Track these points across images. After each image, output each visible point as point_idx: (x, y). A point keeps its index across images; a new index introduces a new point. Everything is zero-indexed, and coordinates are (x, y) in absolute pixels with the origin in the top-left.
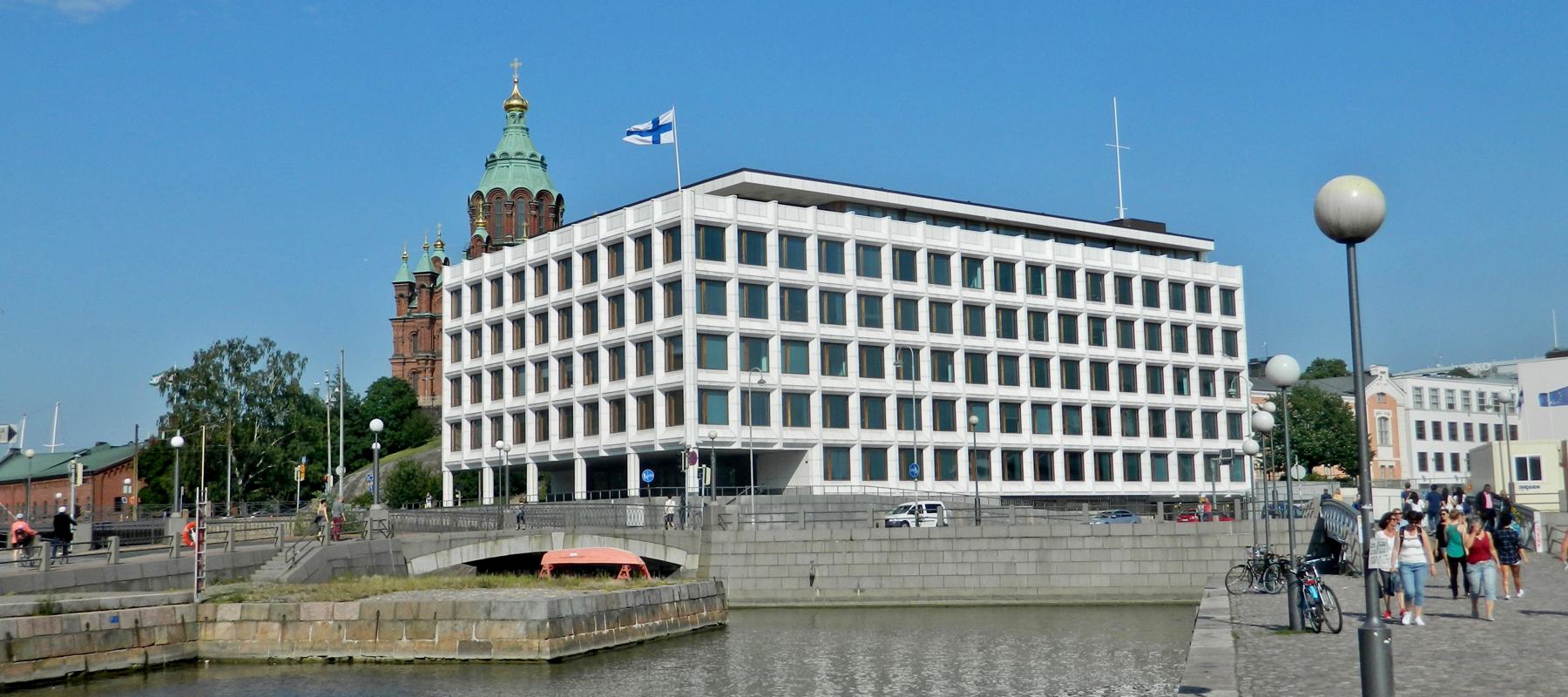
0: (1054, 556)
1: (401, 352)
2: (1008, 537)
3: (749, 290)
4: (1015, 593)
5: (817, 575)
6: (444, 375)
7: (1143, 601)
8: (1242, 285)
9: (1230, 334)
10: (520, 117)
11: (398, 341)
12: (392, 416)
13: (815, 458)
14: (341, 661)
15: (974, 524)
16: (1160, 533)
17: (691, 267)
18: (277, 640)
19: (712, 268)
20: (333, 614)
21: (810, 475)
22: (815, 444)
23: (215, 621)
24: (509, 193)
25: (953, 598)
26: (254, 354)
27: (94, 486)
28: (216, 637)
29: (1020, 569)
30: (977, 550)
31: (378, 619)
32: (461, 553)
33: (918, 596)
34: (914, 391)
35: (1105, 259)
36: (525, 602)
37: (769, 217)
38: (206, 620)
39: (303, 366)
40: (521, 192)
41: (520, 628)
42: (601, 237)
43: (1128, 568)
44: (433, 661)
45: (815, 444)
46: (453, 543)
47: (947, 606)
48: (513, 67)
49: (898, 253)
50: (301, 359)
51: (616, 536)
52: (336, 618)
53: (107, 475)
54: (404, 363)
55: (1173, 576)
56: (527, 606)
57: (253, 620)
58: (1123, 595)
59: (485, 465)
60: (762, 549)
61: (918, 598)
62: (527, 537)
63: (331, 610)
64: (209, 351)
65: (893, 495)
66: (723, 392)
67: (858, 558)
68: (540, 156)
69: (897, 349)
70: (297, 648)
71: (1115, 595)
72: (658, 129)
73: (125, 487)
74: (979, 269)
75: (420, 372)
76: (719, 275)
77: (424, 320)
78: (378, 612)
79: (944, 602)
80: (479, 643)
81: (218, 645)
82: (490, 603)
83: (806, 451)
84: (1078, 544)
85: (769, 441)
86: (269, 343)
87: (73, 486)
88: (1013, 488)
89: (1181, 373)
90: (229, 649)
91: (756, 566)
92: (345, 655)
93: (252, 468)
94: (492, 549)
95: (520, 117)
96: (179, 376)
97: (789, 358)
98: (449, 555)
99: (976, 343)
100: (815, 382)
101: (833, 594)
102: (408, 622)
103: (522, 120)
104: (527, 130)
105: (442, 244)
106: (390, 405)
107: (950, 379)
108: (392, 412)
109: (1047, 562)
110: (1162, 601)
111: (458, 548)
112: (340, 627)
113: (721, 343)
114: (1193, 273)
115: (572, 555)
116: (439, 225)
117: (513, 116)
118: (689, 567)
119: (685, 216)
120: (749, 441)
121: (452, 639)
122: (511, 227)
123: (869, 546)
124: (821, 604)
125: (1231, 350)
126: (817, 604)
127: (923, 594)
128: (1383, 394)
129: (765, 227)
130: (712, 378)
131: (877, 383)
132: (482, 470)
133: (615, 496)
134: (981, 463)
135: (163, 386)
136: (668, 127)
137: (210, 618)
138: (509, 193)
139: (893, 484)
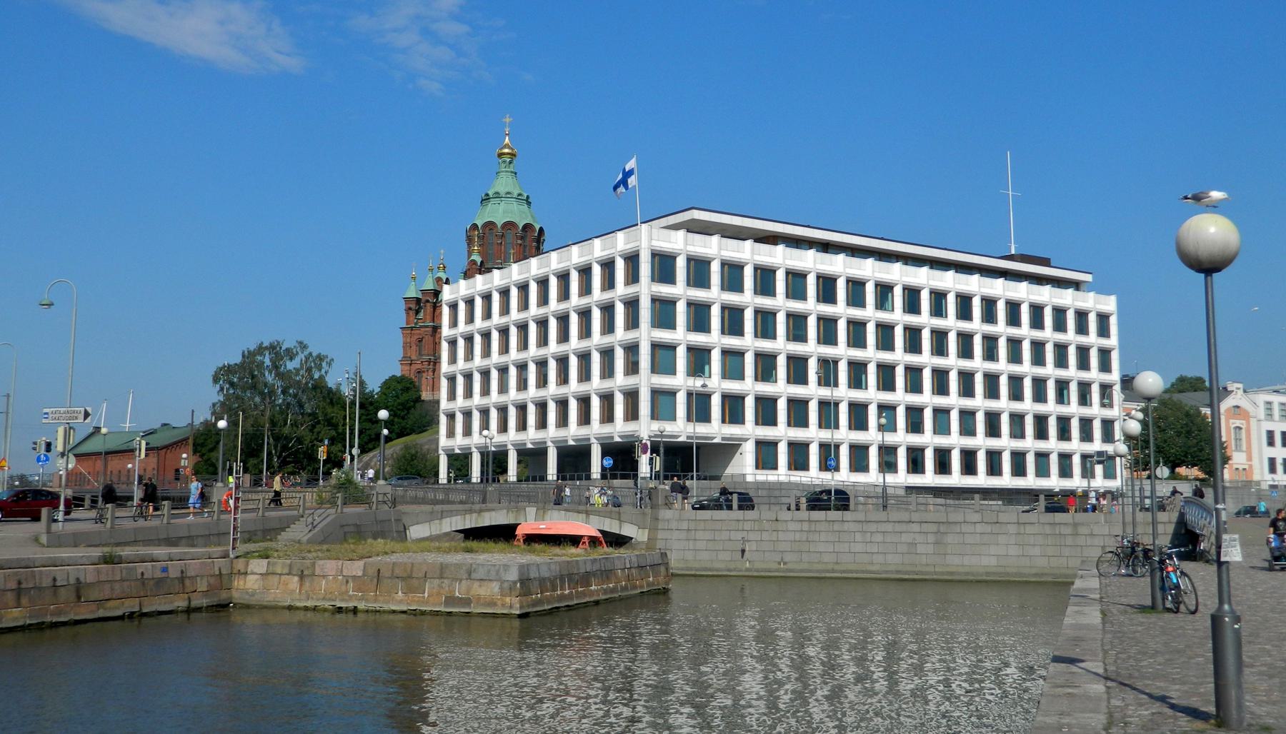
0: (950, 539)
1: (409, 355)
2: (910, 522)
5: (747, 549)
6: (442, 375)
7: (1025, 579)
8: (1116, 312)
9: (1105, 354)
10: (510, 163)
11: (406, 346)
13: (749, 449)
14: (347, 610)
15: (882, 509)
17: (647, 289)
18: (295, 591)
19: (665, 290)
20: (342, 571)
21: (744, 466)
24: (499, 226)
25: (863, 572)
26: (291, 354)
27: (158, 460)
28: (246, 587)
29: (920, 549)
30: (884, 532)
31: (378, 576)
32: (451, 523)
33: (833, 570)
34: (832, 396)
36: (500, 565)
37: (714, 248)
38: (239, 573)
39: (329, 364)
40: (509, 225)
41: (495, 587)
42: (574, 262)
43: (1013, 551)
44: (423, 613)
46: (444, 514)
47: (856, 579)
48: (506, 122)
49: (821, 279)
51: (579, 512)
52: (345, 574)
53: (169, 451)
54: (411, 364)
55: (1052, 559)
57: (278, 574)
58: (1008, 574)
60: (702, 525)
61: (833, 571)
62: (505, 511)
63: (340, 567)
65: (813, 483)
66: (672, 393)
67: (782, 536)
68: (525, 195)
69: (819, 360)
70: (312, 598)
71: (1001, 573)
73: (183, 461)
74: (890, 295)
75: (424, 372)
76: (671, 296)
77: (427, 329)
78: (379, 570)
79: (855, 575)
80: (461, 598)
81: (247, 593)
82: (471, 565)
86: (303, 346)
87: (137, 458)
88: (916, 480)
89: (1062, 386)
91: (695, 540)
92: (351, 605)
93: (285, 448)
94: (477, 519)
95: (510, 163)
98: (440, 524)
99: (886, 356)
100: (749, 386)
101: (758, 565)
102: (403, 579)
103: (511, 165)
104: (516, 174)
106: (398, 398)
107: (864, 387)
108: (399, 404)
109: (944, 544)
110: (1042, 580)
111: (448, 519)
113: (671, 352)
114: (1073, 300)
115: (541, 527)
117: (504, 162)
118: (640, 539)
119: (643, 246)
120: (692, 435)
121: (439, 594)
123: (792, 526)
124: (750, 574)
125: (1105, 366)
126: (747, 574)
127: (837, 567)
128: (1238, 407)
130: (664, 381)
131: (802, 389)
132: (471, 454)
133: (580, 479)
136: (631, 173)
137: (242, 571)
138: (499, 226)
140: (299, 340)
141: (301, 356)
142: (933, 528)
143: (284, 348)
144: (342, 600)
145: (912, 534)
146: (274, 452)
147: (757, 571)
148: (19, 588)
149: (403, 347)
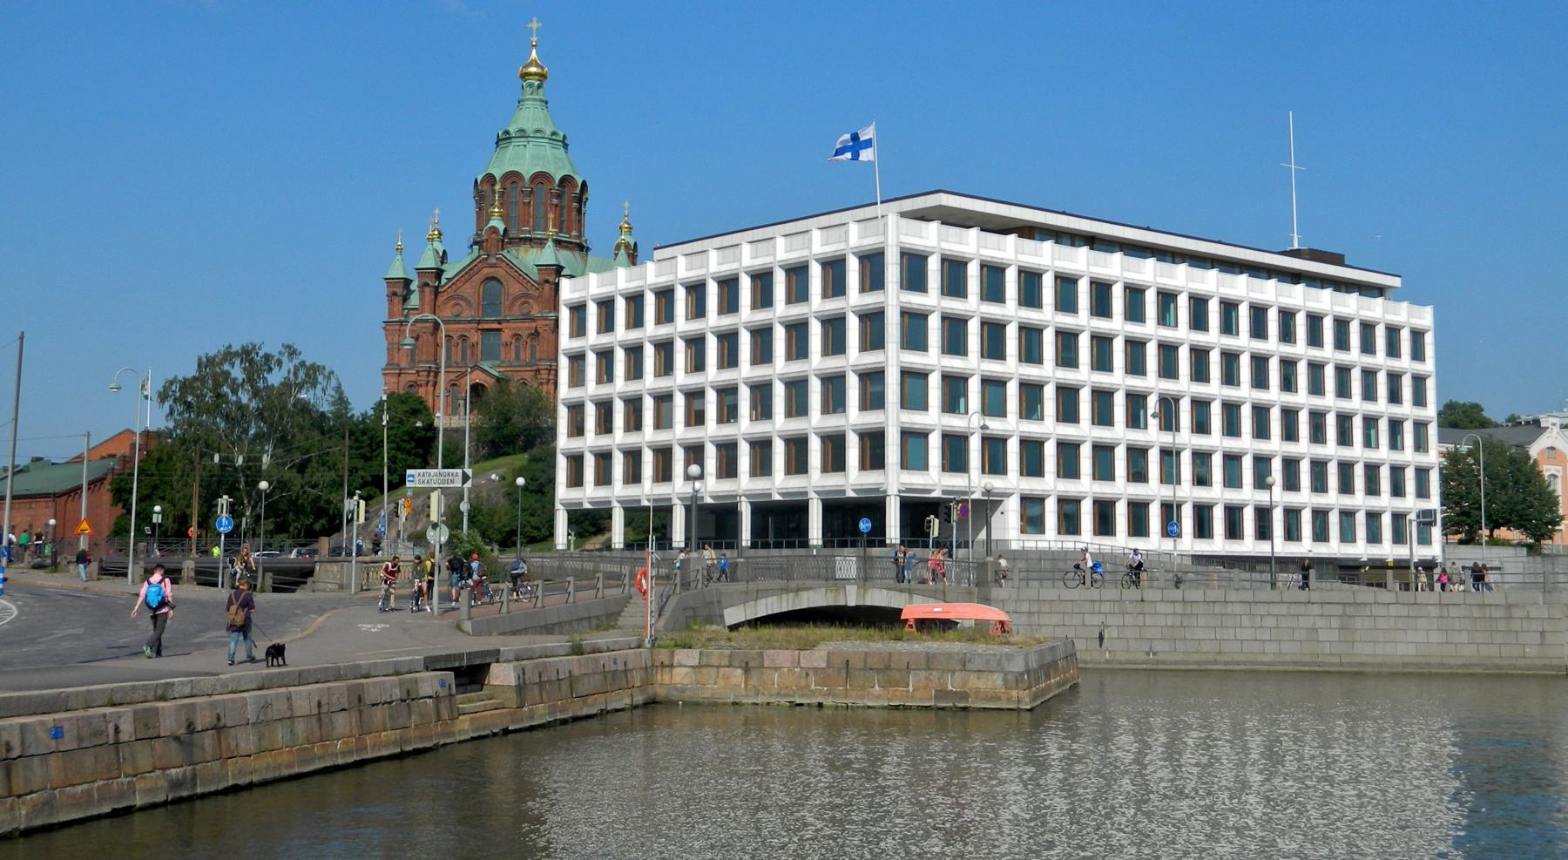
0: (1358, 623)
1: (396, 361)
2: (1309, 602)
3: (950, 327)
4: (1317, 660)
5: (1106, 636)
8: (1432, 328)
9: (1419, 381)
10: (539, 87)
12: (406, 438)
13: (1012, 506)
15: (1269, 588)
16: (1468, 602)
17: (893, 298)
18: (739, 686)
19: (915, 300)
20: (799, 662)
21: (1008, 526)
22: (1011, 494)
23: (672, 666)
24: (527, 177)
25: (1252, 663)
29: (1322, 635)
33: (1215, 661)
35: (1270, 292)
36: (1001, 655)
37: (973, 245)
40: (541, 177)
41: (997, 680)
42: (778, 258)
43: (1435, 637)
45: (1012, 494)
46: (760, 593)
48: (532, 29)
49: (1023, 275)
50: (327, 373)
52: (802, 665)
54: (399, 374)
56: (1004, 658)
58: (1429, 665)
59: (615, 504)
60: (1046, 608)
61: (1215, 662)
62: (823, 590)
64: (216, 356)
67: (1149, 620)
70: (763, 694)
72: (856, 145)
74: (1172, 306)
75: (421, 385)
77: (427, 325)
81: (676, 688)
83: (1002, 501)
84: (1382, 611)
85: (928, 487)
86: (292, 352)
87: (355, 523)
90: (689, 693)
92: (815, 701)
94: (794, 600)
95: (539, 87)
96: (186, 385)
97: (987, 401)
98: (755, 606)
100: (1012, 425)
101: (1120, 656)
102: (878, 670)
103: (541, 91)
104: (546, 103)
105: (440, 234)
107: (1142, 426)
108: (407, 433)
111: (763, 601)
112: (807, 674)
113: (920, 381)
114: (1384, 313)
115: (936, 610)
116: (437, 212)
117: (531, 85)
119: (890, 243)
121: (926, 688)
122: (529, 218)
123: (1161, 608)
124: (1111, 666)
125: (1419, 400)
127: (1219, 658)
128: (1552, 448)
129: (967, 256)
130: (915, 419)
133: (790, 545)
134: (1033, 511)
135: (163, 397)
136: (868, 144)
137: (666, 663)
138: (527, 177)
139: (1121, 540)
140: (286, 343)
141: (288, 365)
142: (1338, 610)
143: (261, 353)
144: (803, 696)
145: (1312, 618)
146: (246, 502)
147: (1120, 663)
148: (540, 682)
149: (388, 349)
